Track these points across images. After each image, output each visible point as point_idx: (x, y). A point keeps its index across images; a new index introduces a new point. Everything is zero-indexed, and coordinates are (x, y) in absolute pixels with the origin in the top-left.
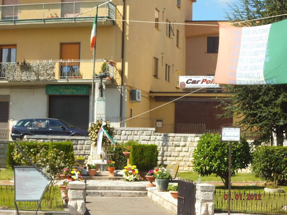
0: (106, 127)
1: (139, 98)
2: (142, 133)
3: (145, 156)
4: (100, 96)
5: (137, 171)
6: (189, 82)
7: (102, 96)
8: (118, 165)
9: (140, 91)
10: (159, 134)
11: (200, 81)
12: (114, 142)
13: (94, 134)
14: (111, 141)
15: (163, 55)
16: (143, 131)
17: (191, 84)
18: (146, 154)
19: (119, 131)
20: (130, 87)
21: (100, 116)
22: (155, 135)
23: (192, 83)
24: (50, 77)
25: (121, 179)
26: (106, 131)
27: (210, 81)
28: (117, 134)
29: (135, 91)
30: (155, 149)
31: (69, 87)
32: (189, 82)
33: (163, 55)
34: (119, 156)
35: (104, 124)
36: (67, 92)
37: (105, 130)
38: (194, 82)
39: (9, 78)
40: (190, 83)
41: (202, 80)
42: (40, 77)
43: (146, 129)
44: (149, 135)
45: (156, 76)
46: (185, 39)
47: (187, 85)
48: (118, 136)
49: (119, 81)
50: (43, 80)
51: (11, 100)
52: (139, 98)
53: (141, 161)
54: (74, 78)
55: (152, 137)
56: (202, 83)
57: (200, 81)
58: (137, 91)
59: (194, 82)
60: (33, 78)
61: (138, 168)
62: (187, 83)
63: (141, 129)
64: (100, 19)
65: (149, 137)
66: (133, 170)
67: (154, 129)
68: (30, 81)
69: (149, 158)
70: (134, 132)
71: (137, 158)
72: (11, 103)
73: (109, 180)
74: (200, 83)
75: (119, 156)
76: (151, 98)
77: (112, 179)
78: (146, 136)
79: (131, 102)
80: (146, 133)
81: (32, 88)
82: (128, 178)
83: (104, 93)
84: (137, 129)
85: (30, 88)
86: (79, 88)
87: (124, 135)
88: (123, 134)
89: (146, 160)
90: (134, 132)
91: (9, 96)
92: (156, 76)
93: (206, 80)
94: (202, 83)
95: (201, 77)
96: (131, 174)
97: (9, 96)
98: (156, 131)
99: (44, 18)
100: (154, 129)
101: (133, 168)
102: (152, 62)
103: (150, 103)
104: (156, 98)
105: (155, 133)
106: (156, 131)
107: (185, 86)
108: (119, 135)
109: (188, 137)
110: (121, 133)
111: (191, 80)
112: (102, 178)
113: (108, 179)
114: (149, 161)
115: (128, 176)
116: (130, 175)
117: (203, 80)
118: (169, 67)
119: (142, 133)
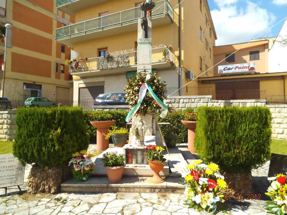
0: (151, 83)
1: (192, 78)
2: (199, 101)
3: (240, 139)
4: (144, 37)
5: (222, 183)
6: (225, 69)
7: (146, 36)
8: (175, 141)
9: (193, 73)
10: (216, 101)
11: (233, 68)
12: (164, 106)
13: (133, 93)
14: (161, 106)
15: (204, 58)
16: (200, 99)
17: (227, 71)
18: (242, 130)
19: (177, 99)
20: (186, 69)
21: (144, 67)
22: (212, 102)
23: (228, 70)
24: (126, 64)
25: (178, 191)
26: (152, 88)
27: (241, 67)
28: (176, 102)
29: (190, 71)
30: (266, 118)
32: (225, 69)
33: (204, 58)
34: (177, 124)
35: (148, 77)
37: (150, 88)
38: (229, 69)
39: (100, 67)
40: (226, 70)
41: (235, 67)
42: (119, 65)
43: (203, 96)
44: (206, 102)
45: (201, 69)
46: (213, 56)
47: (224, 71)
48: (177, 104)
49: (177, 65)
50: (122, 67)
51: (105, 84)
52: (192, 78)
53: (230, 150)
55: (209, 104)
56: (235, 69)
57: (233, 68)
58: (191, 72)
59: (229, 69)
60: (115, 66)
61: (223, 169)
62: (224, 70)
63: (198, 97)
64: (161, 15)
65: (206, 104)
66: (212, 178)
67: (211, 96)
68: (113, 68)
70: (191, 100)
71: (217, 143)
72: (105, 86)
73: (151, 192)
74: (233, 69)
75: (177, 124)
76: (199, 82)
77: (157, 190)
78: (204, 104)
79: (187, 80)
80: (203, 100)
81: (118, 76)
82: (198, 199)
83: (150, 33)
84: (195, 97)
85: (116, 75)
87: (182, 103)
88: (181, 102)
89: (245, 147)
90: (191, 100)
91: (104, 82)
92: (201, 69)
93: (238, 67)
94: (235, 69)
95: (234, 65)
96: (205, 189)
97: (104, 82)
98: (212, 99)
100: (211, 96)
101: (209, 172)
102: (199, 59)
103: (198, 84)
104: (202, 82)
105: (212, 100)
106: (212, 99)
107: (222, 72)
109: (247, 103)
110: (179, 102)
111: (227, 68)
112: (134, 188)
113: (148, 190)
114: (251, 150)
115: (196, 194)
116: (203, 192)
117: (236, 67)
118: (207, 67)
119: (199, 101)
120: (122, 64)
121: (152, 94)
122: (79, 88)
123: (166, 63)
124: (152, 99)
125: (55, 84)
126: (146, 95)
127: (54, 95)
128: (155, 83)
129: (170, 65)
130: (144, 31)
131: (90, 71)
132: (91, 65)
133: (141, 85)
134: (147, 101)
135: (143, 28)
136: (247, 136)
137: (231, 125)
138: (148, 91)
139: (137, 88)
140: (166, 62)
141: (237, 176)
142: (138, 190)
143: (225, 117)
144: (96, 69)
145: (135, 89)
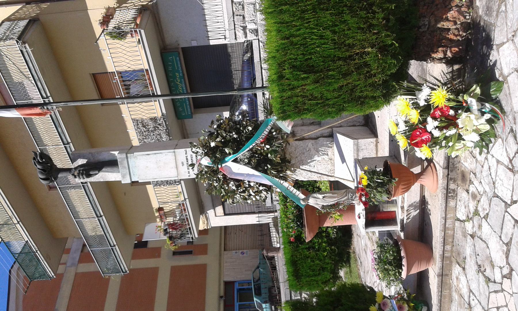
3: (338, 45)
4: (115, 169)
7: (113, 164)
19: (234, 10)
24: (159, 125)
28: (241, 12)
31: (172, 84)
36: (182, 87)
48: (246, 10)
53: (366, 65)
54: (152, 87)
69: (352, 21)
83: (104, 156)
86: (170, 68)
89: (359, 36)
99: (62, 144)
108: (243, 8)
112: (445, 229)
113: (452, 203)
115: (460, 138)
120: (160, 135)
121: (243, 153)
122: (225, 214)
123: (142, 31)
124: (253, 152)
125: (220, 255)
126: (248, 164)
127: (245, 255)
128: (216, 147)
129: (147, 14)
130: (104, 169)
131: (185, 199)
132: (172, 199)
133: (225, 176)
134: (259, 162)
135: (97, 172)
136: (334, 32)
137: (310, 69)
138: (235, 161)
139: (232, 186)
140: (140, 31)
141: (425, 25)
142: (449, 222)
143: (295, 83)
144: (180, 186)
145: (234, 188)
